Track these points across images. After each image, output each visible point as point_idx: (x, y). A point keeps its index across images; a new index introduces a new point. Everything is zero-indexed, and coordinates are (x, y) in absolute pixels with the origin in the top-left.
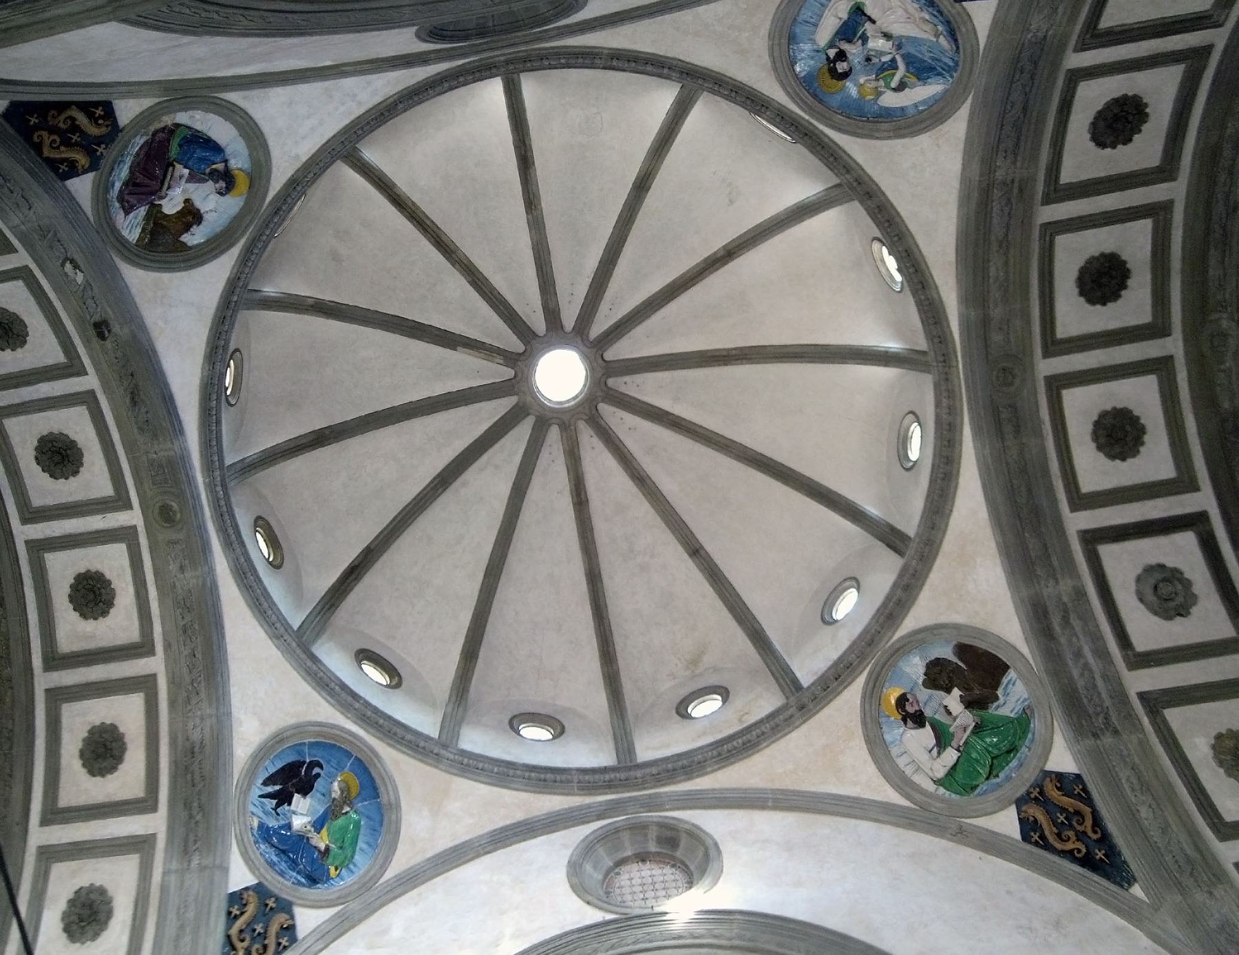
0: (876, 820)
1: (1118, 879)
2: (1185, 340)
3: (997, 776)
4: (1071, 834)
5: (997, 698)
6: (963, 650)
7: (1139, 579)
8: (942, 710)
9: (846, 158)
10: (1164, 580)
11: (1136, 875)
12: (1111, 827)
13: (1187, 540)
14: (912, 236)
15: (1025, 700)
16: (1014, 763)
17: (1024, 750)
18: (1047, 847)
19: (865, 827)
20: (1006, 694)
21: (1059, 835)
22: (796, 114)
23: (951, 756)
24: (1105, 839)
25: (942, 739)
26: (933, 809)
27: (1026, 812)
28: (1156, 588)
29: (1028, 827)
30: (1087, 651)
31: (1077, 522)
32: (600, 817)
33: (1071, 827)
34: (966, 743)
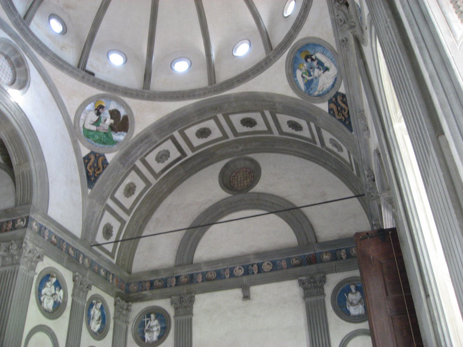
0: (64, 118)
1: (89, 185)
2: (234, 140)
3: (95, 143)
4: (93, 169)
5: (116, 132)
6: (126, 118)
7: (164, 150)
8: (105, 119)
9: (278, 57)
10: (166, 155)
11: (93, 189)
12: (100, 178)
13: (178, 154)
14: (254, 78)
15: (120, 140)
16: (101, 145)
17: (106, 146)
18: (86, 166)
19: (60, 116)
20: (119, 135)
21: (90, 167)
22: (292, 43)
23: (94, 128)
24: (96, 178)
25: (97, 123)
26: (76, 131)
27: (91, 156)
28: (163, 155)
29: (87, 159)
30: (141, 150)
31: (176, 134)
32: (10, 35)
33: (95, 169)
34: (100, 132)
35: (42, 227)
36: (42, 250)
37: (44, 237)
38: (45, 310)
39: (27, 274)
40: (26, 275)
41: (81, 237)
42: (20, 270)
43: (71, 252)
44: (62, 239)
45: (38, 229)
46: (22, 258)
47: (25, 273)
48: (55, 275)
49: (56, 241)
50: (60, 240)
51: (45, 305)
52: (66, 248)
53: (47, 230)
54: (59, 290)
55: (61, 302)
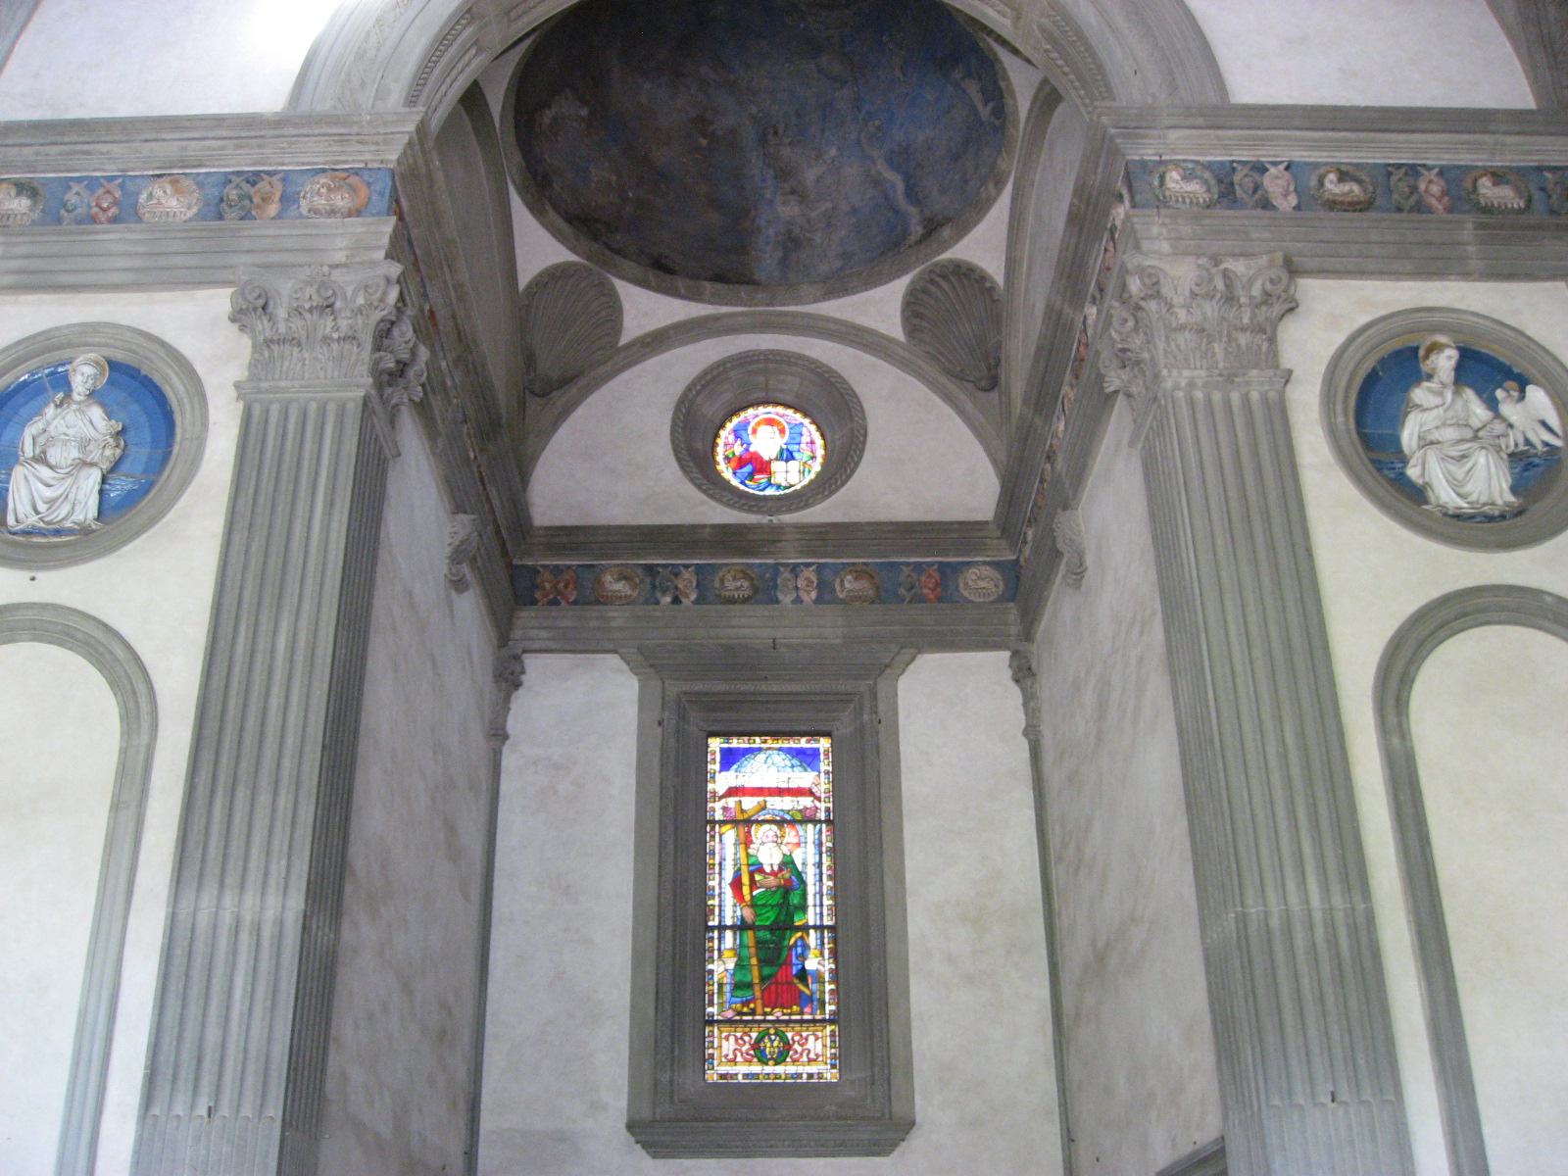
35: (1234, 169)
36: (1264, 260)
37: (1266, 204)
38: (1457, 517)
39: (1235, 397)
40: (1227, 403)
41: (1537, 104)
42: (1180, 394)
43: (1487, 189)
44: (1399, 166)
45: (1208, 190)
46: (1161, 346)
47: (1217, 397)
48: (1442, 339)
49: (1356, 188)
50: (1390, 174)
51: (1444, 494)
52: (1444, 193)
53: (1273, 170)
54: (1515, 394)
55: (1558, 443)
